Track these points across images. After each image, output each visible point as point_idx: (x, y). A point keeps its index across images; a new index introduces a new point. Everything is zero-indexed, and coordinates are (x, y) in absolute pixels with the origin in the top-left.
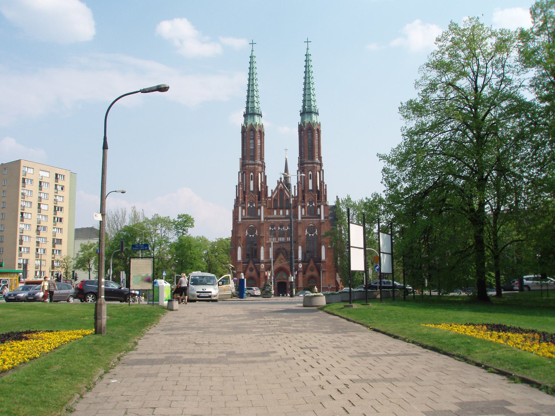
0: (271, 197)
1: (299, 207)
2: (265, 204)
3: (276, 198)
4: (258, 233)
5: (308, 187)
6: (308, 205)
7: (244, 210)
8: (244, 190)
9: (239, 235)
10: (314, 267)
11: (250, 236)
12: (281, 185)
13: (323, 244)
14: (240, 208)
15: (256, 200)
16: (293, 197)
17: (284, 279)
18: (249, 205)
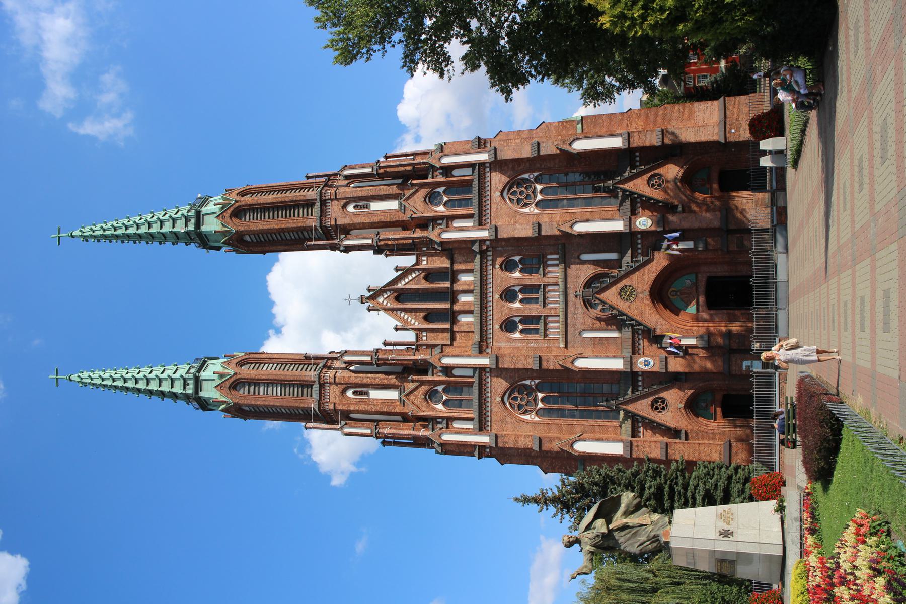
0: (418, 331)
1: (447, 236)
2: (436, 351)
3: (422, 314)
4: (532, 379)
5: (390, 211)
6: (441, 208)
7: (456, 425)
8: (399, 418)
9: (536, 448)
10: (649, 175)
11: (540, 405)
12: (380, 300)
13: (566, 147)
14: (447, 437)
15: (422, 383)
16: (418, 262)
17: (696, 284)
18: (440, 407)
